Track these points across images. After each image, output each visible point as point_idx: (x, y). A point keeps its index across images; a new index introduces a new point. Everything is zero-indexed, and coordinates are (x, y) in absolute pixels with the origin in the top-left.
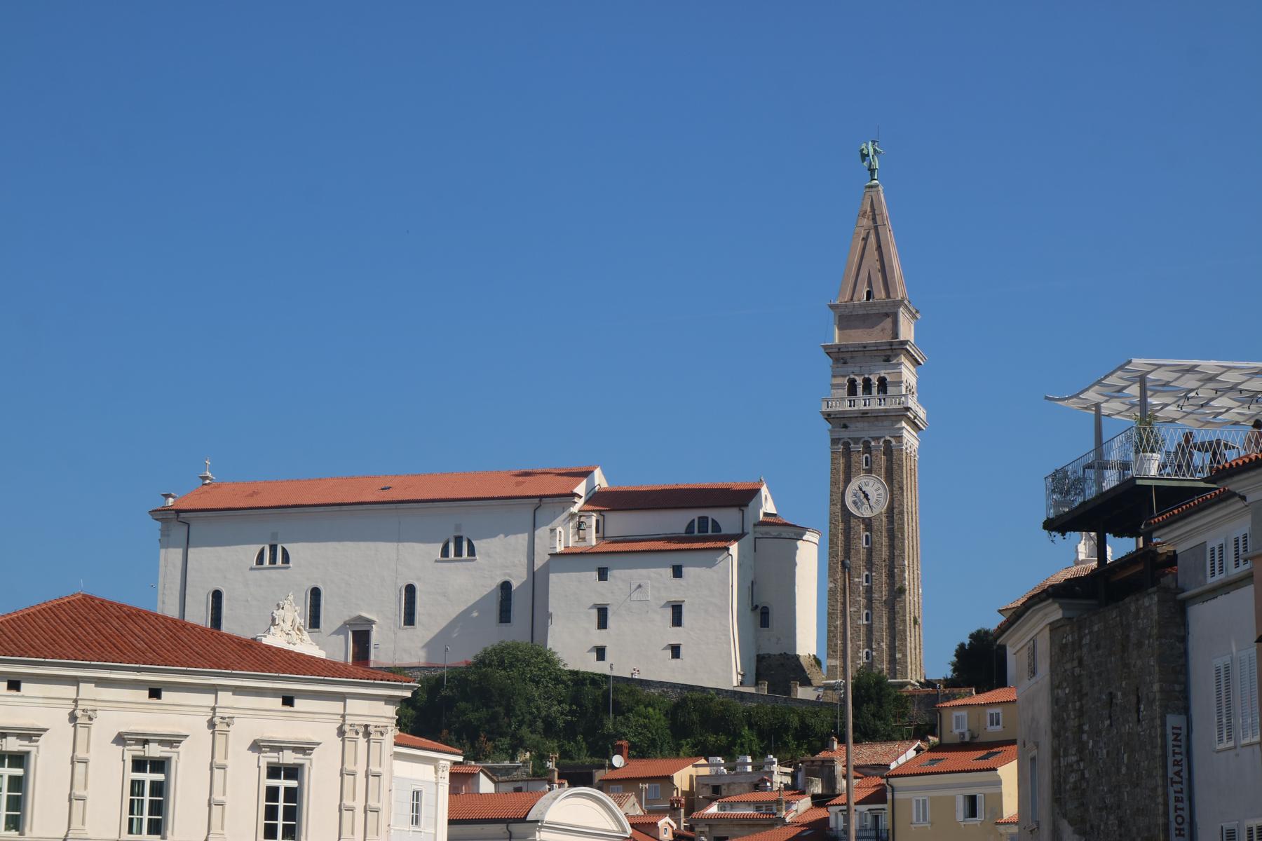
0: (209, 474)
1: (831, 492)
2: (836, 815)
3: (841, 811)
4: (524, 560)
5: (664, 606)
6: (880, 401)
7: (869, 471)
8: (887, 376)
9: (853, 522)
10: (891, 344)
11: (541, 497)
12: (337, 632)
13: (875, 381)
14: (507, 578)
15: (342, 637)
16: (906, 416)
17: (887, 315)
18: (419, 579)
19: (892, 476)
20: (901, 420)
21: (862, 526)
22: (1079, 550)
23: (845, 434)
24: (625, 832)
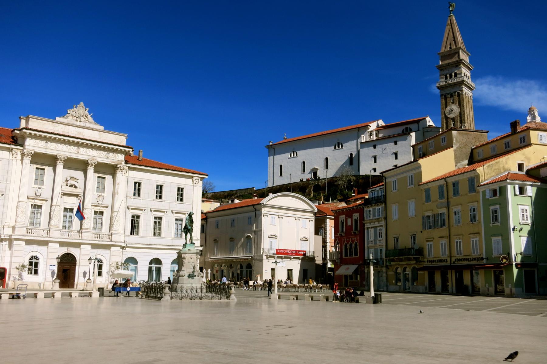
0: (285, 137)
1: (441, 111)
2: (370, 193)
3: (371, 191)
4: (356, 146)
5: (392, 154)
6: (455, 79)
7: (453, 103)
8: (457, 72)
9: (449, 120)
10: (457, 61)
11: (359, 128)
12: (309, 173)
13: (453, 74)
14: (351, 152)
15: (310, 174)
16: (464, 83)
17: (456, 53)
18: (329, 156)
19: (461, 104)
20: (462, 85)
21: (451, 121)
22: (528, 119)
23: (444, 93)
24: (314, 210)
